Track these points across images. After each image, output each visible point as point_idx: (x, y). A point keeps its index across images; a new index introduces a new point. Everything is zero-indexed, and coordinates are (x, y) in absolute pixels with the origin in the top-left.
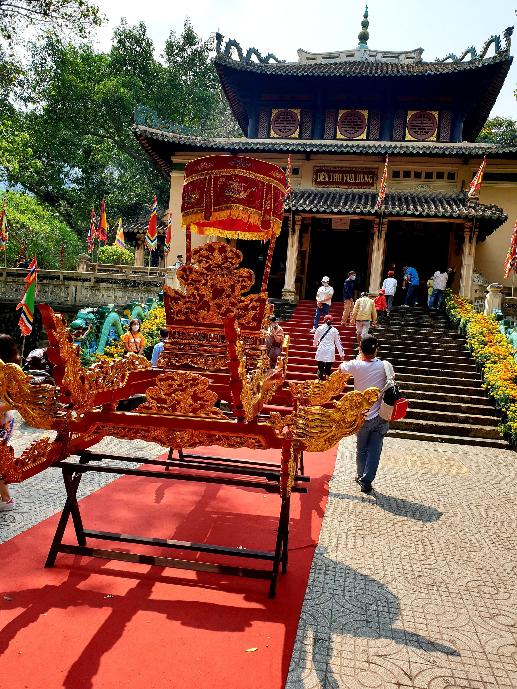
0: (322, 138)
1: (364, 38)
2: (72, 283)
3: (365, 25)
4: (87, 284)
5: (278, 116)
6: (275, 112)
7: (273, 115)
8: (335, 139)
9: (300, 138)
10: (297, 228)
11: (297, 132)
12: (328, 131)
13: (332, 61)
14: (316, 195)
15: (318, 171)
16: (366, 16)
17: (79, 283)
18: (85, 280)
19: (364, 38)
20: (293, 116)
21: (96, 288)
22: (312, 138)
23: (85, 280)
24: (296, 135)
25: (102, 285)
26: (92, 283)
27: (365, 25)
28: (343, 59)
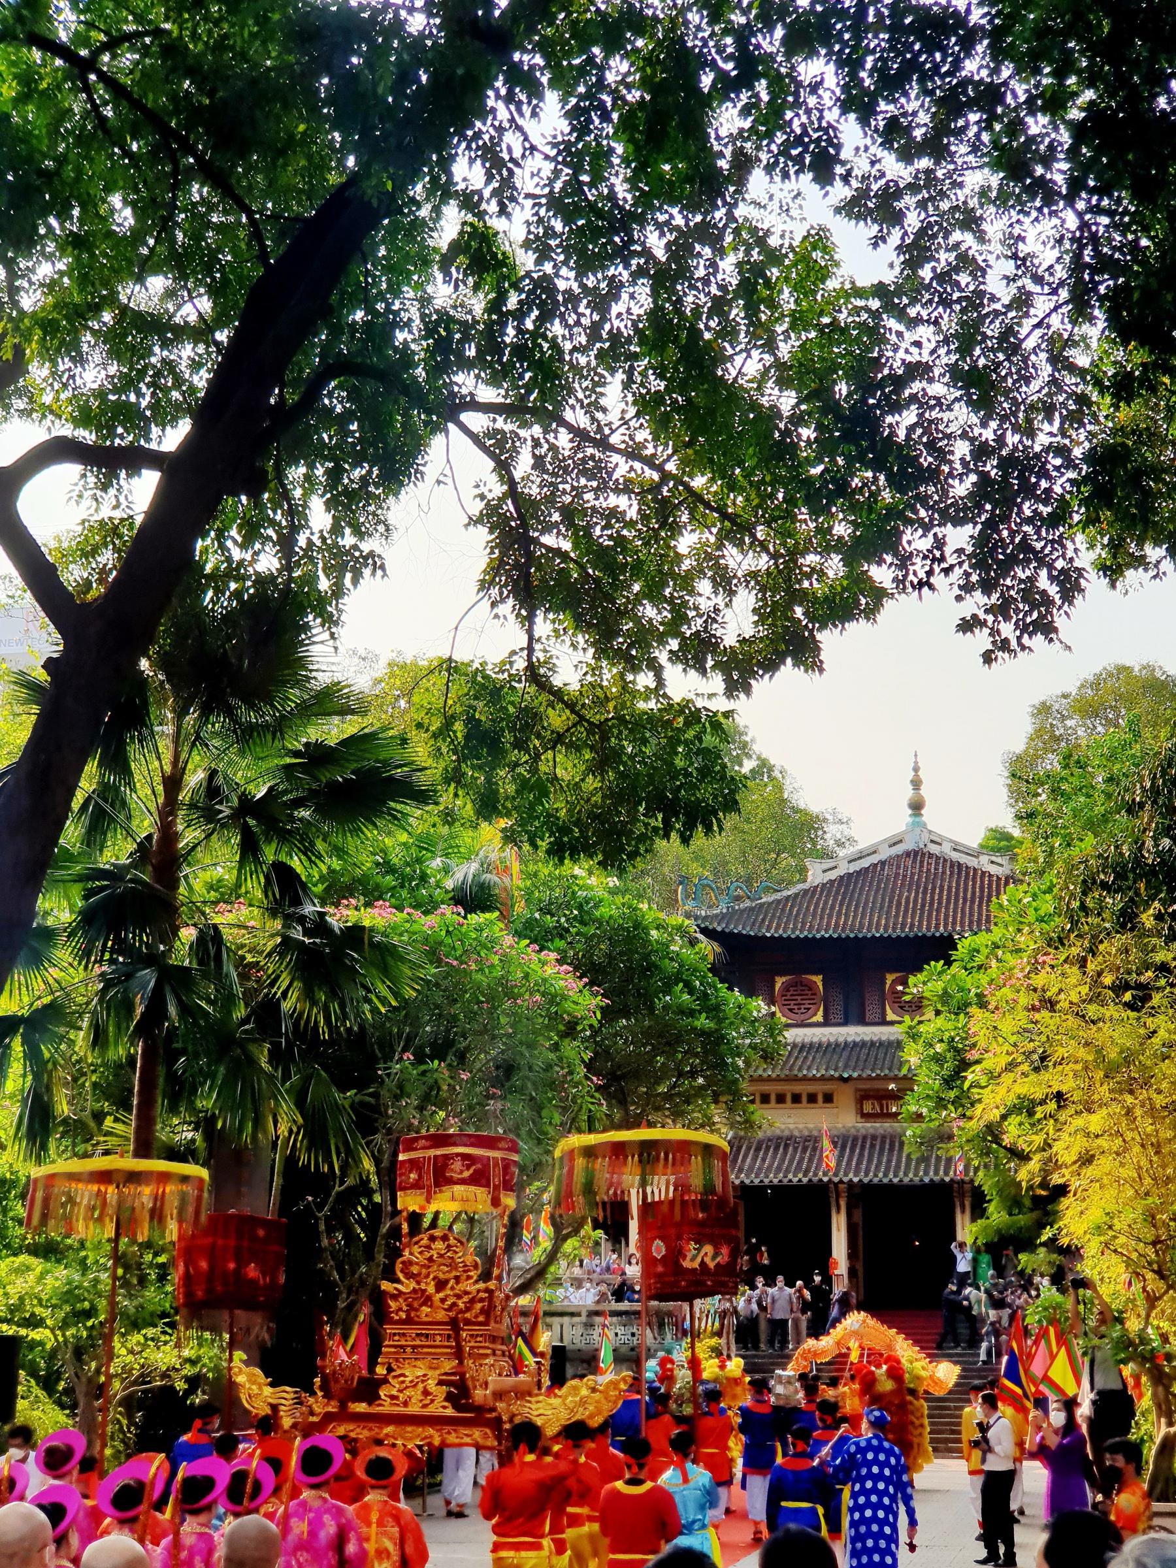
0: (862, 1021)
1: (917, 807)
2: (556, 1321)
3: (916, 783)
4: (576, 1319)
5: (786, 988)
6: (779, 982)
7: (778, 986)
8: (884, 1022)
9: (826, 1023)
10: (843, 1203)
11: (821, 1012)
12: (871, 1012)
13: (865, 863)
14: (865, 1138)
15: (863, 1097)
16: (916, 769)
17: (566, 1320)
18: (572, 1314)
19: (917, 807)
20: (811, 986)
21: (589, 1325)
22: (845, 1023)
23: (572, 1314)
24: (819, 1017)
25: (598, 1320)
26: (583, 1318)
27: (916, 783)
28: (885, 854)
